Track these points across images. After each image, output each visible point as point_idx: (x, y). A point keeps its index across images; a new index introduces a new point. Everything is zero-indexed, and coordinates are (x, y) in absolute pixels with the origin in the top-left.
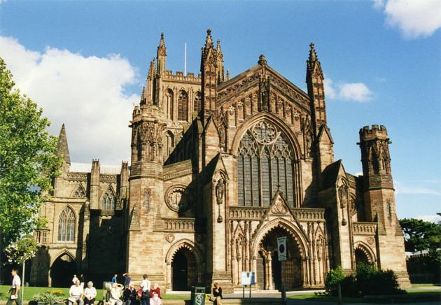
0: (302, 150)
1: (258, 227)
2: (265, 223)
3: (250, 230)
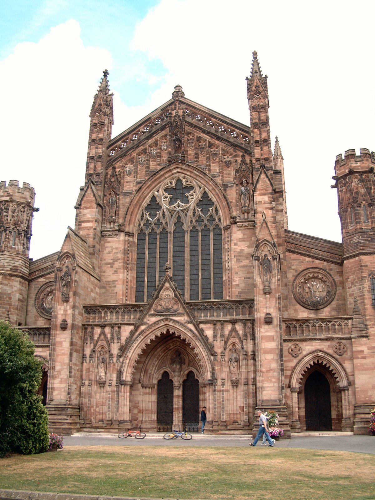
0: (233, 209)
1: (132, 333)
2: (143, 327)
3: (119, 339)
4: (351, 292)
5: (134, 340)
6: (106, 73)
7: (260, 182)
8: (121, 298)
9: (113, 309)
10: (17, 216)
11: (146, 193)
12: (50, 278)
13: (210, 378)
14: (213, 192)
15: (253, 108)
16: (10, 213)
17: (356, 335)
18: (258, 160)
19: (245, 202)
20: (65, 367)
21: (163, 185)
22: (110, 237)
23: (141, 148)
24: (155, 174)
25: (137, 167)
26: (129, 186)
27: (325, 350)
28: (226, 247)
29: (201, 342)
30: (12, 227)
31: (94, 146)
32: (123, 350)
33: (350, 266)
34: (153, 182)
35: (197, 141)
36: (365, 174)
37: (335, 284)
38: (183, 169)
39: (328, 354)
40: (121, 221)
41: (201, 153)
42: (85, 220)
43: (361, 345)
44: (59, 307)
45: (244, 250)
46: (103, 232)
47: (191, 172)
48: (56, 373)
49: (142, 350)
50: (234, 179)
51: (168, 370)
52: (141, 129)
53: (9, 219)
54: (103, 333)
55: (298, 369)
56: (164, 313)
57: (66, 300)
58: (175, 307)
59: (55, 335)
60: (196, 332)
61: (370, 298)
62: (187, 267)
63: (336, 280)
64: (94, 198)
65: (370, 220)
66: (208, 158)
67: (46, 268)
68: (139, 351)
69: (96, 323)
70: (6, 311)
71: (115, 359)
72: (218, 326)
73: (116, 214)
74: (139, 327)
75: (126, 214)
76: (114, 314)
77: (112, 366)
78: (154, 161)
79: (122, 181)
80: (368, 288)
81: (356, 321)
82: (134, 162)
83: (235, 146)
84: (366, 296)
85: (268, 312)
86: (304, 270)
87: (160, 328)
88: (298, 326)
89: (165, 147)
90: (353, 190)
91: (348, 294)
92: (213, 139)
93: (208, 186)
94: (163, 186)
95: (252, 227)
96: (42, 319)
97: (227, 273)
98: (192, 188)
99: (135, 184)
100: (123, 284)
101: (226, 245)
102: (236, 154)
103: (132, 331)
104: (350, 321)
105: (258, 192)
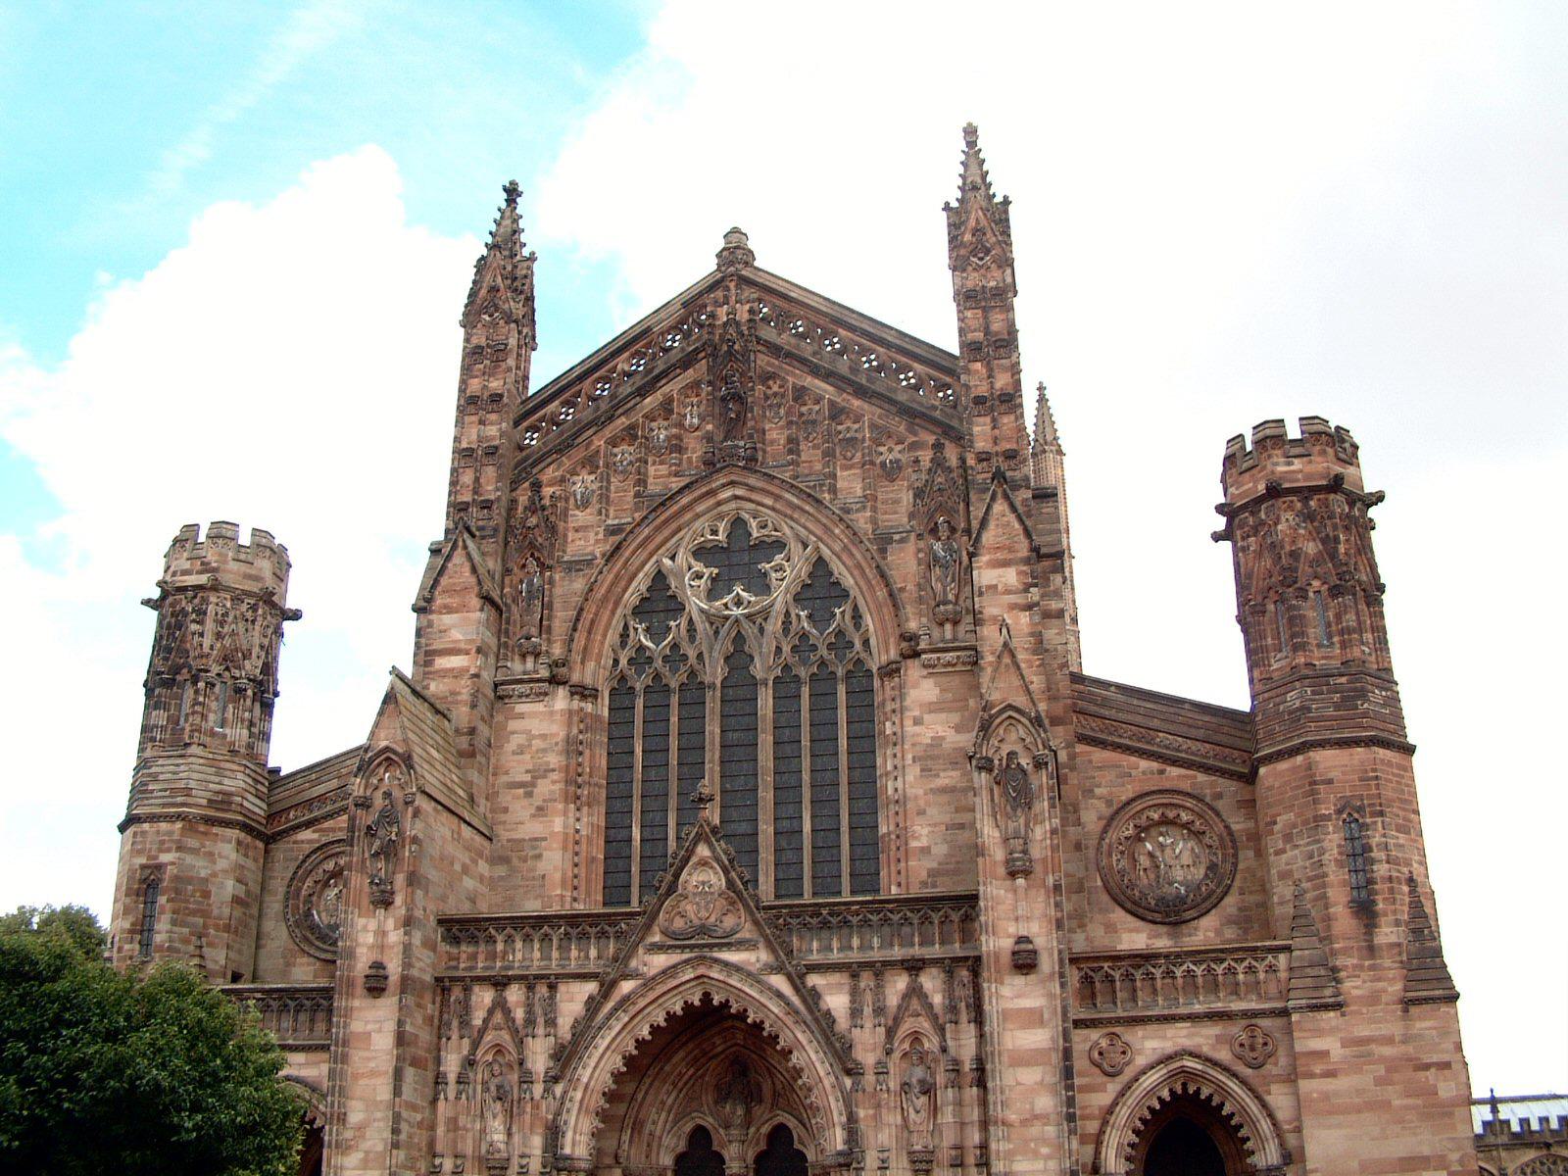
0: (909, 610)
1: (593, 1005)
2: (627, 987)
3: (551, 1022)
4: (1283, 867)
5: (600, 1028)
6: (512, 193)
7: (992, 525)
8: (559, 892)
9: (533, 927)
10: (233, 633)
11: (636, 561)
12: (333, 830)
13: (840, 1147)
14: (844, 557)
15: (966, 298)
16: (210, 626)
17: (1304, 1001)
18: (984, 457)
19: (945, 588)
20: (379, 1115)
21: (687, 539)
22: (524, 699)
23: (619, 422)
24: (663, 504)
25: (609, 482)
26: (582, 542)
27: (1206, 1050)
28: (889, 729)
29: (812, 1032)
30: (215, 669)
31: (474, 418)
32: (565, 1057)
33: (1277, 784)
34: (658, 529)
35: (795, 400)
36: (1316, 497)
37: (1233, 841)
38: (752, 489)
39: (1215, 1064)
40: (557, 651)
41: (807, 438)
42: (446, 649)
43: (1320, 1033)
44: (361, 922)
45: (943, 738)
46: (502, 684)
47: (777, 498)
48: (348, 1134)
49: (624, 1058)
50: (911, 516)
51: (708, 1122)
52: (622, 364)
53: (207, 642)
54: (500, 1004)
55: (1123, 1114)
56: (692, 942)
57: (385, 901)
58: (729, 922)
59: (348, 1013)
60: (795, 1000)
61: (1344, 883)
62: (766, 795)
63: (1235, 827)
64: (473, 580)
65: (1336, 639)
66: (829, 454)
67: (321, 798)
68: (617, 1062)
69: (479, 972)
70: (192, 934)
71: (538, 1089)
72: (866, 980)
73: (544, 628)
74: (614, 984)
75: (575, 629)
76: (537, 946)
77: (529, 1110)
78: (661, 463)
79: (561, 525)
80: (1335, 851)
81: (1301, 958)
82: (598, 467)
83: (914, 415)
84: (1332, 878)
85: (1023, 932)
86: (1133, 800)
87: (681, 989)
88: (1117, 975)
89: (695, 421)
90: (1282, 547)
91: (1274, 871)
92: (845, 395)
93: (829, 542)
94: (688, 540)
95: (969, 668)
96: (305, 960)
97: (891, 813)
98: (779, 545)
99: (601, 536)
100: (565, 848)
101: (888, 724)
102: (914, 439)
103: (591, 998)
104: (1282, 958)
105: (985, 559)
